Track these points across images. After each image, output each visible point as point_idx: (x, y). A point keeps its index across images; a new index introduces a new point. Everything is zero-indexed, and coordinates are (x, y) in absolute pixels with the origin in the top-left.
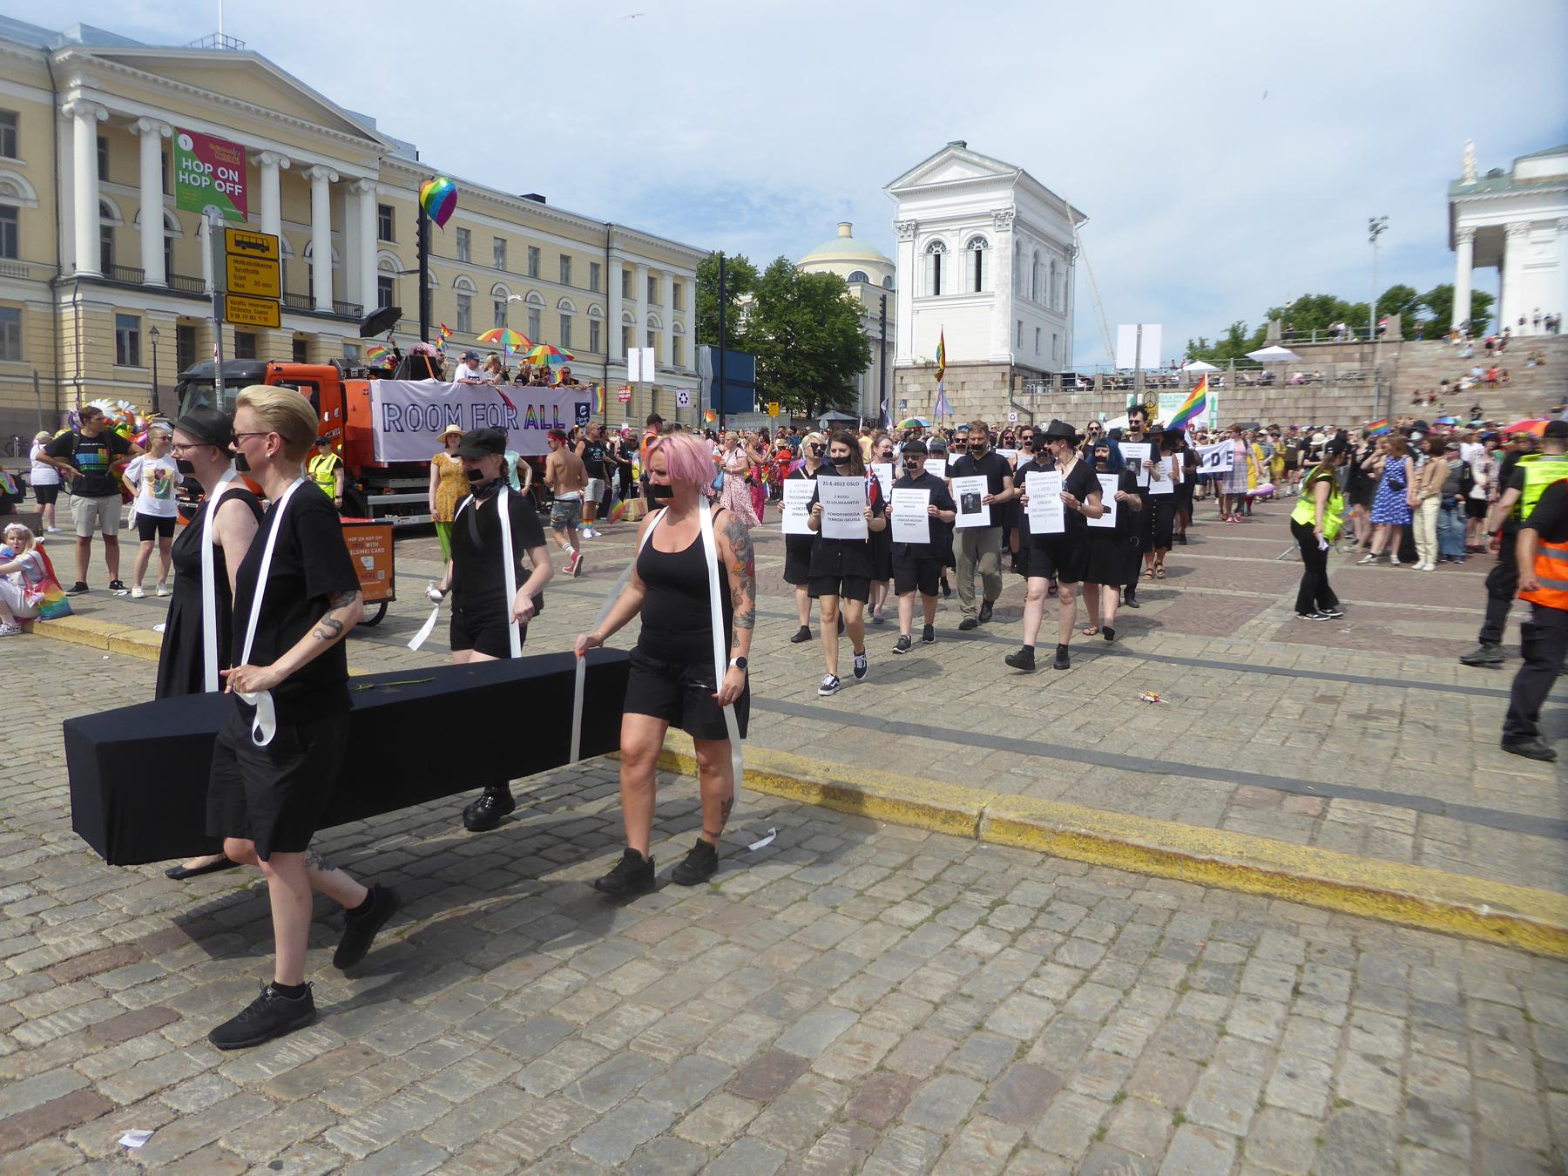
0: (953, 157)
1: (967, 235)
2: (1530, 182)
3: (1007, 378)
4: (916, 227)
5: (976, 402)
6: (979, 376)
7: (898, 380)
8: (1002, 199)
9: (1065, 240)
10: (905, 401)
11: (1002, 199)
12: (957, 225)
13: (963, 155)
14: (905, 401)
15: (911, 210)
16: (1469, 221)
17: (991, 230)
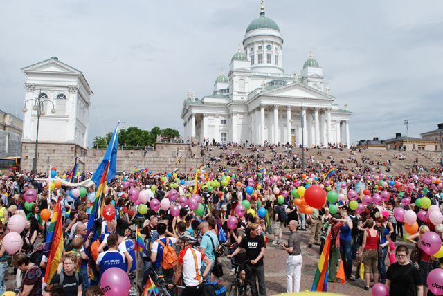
0: (54, 63)
1: (57, 93)
2: (208, 103)
3: (74, 149)
4: (32, 87)
5: (60, 158)
6: (62, 148)
7: (23, 148)
8: (74, 82)
9: (87, 100)
10: (27, 157)
11: (74, 82)
12: (54, 89)
13: (56, 62)
14: (27, 157)
15: (32, 80)
16: (195, 111)
17: (67, 92)
